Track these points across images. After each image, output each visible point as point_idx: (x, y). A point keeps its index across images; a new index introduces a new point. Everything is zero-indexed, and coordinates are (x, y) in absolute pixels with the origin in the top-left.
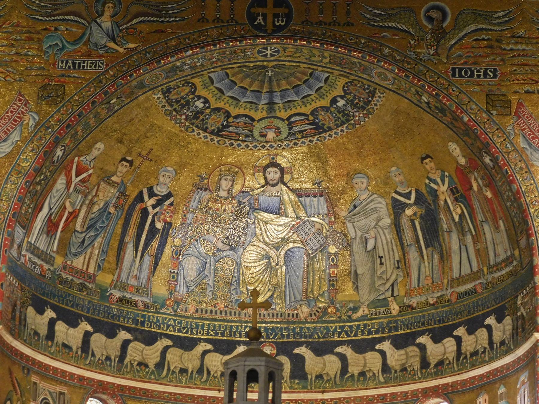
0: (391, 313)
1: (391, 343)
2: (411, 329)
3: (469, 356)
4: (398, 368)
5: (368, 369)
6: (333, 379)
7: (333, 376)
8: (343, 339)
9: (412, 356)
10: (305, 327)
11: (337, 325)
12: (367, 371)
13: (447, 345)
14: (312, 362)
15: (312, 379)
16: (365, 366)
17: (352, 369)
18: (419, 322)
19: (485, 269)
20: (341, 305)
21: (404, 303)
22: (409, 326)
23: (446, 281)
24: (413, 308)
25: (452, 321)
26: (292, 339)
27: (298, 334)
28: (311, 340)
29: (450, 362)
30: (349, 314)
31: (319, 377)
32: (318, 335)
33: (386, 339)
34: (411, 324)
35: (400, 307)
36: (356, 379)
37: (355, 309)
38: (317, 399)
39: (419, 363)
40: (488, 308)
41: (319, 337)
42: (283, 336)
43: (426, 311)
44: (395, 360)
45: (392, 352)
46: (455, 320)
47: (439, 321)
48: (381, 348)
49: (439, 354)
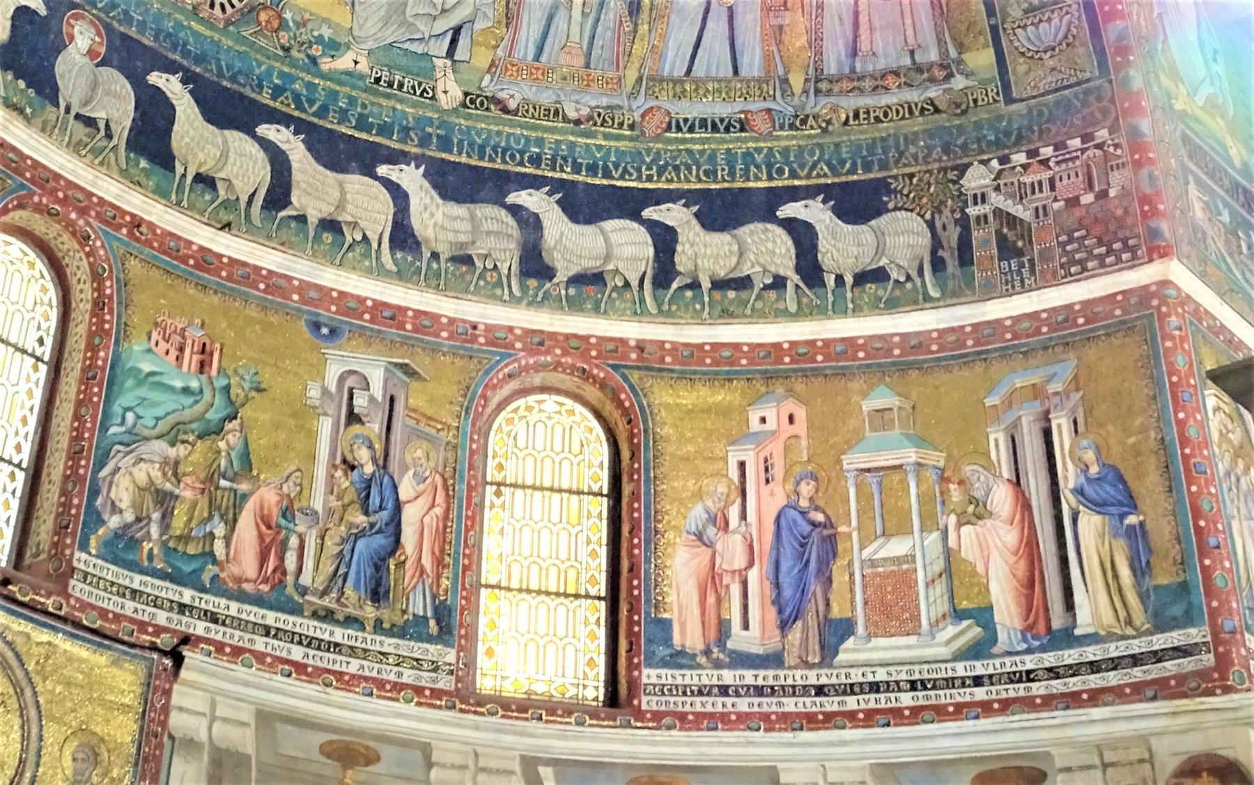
0: (433, 98)
1: (424, 175)
2: (492, 160)
3: (706, 284)
4: (445, 252)
5: (349, 219)
6: (243, 206)
7: (244, 199)
8: (284, 109)
9: (489, 233)
10: (190, 28)
11: (277, 64)
12: (346, 223)
13: (614, 238)
14: (192, 132)
15: (184, 176)
16: (341, 206)
17: (304, 200)
18: (522, 153)
19: (797, 81)
20: (298, 19)
21: (480, 88)
22: (488, 150)
23: (631, 75)
24: (505, 110)
25: (639, 179)
26: (148, 41)
27: (169, 35)
28: (198, 70)
29: (627, 284)
30: (313, 52)
31: (206, 181)
32: (220, 67)
33: (412, 159)
34: (494, 149)
35: (466, 94)
36: (312, 234)
37: (334, 47)
38: (191, 243)
39: (516, 260)
40: (794, 175)
41: (220, 74)
42: (128, 19)
43: (547, 130)
44: (435, 224)
45: (428, 201)
46: (649, 179)
47: (592, 169)
48: (394, 178)
49: (585, 253)
